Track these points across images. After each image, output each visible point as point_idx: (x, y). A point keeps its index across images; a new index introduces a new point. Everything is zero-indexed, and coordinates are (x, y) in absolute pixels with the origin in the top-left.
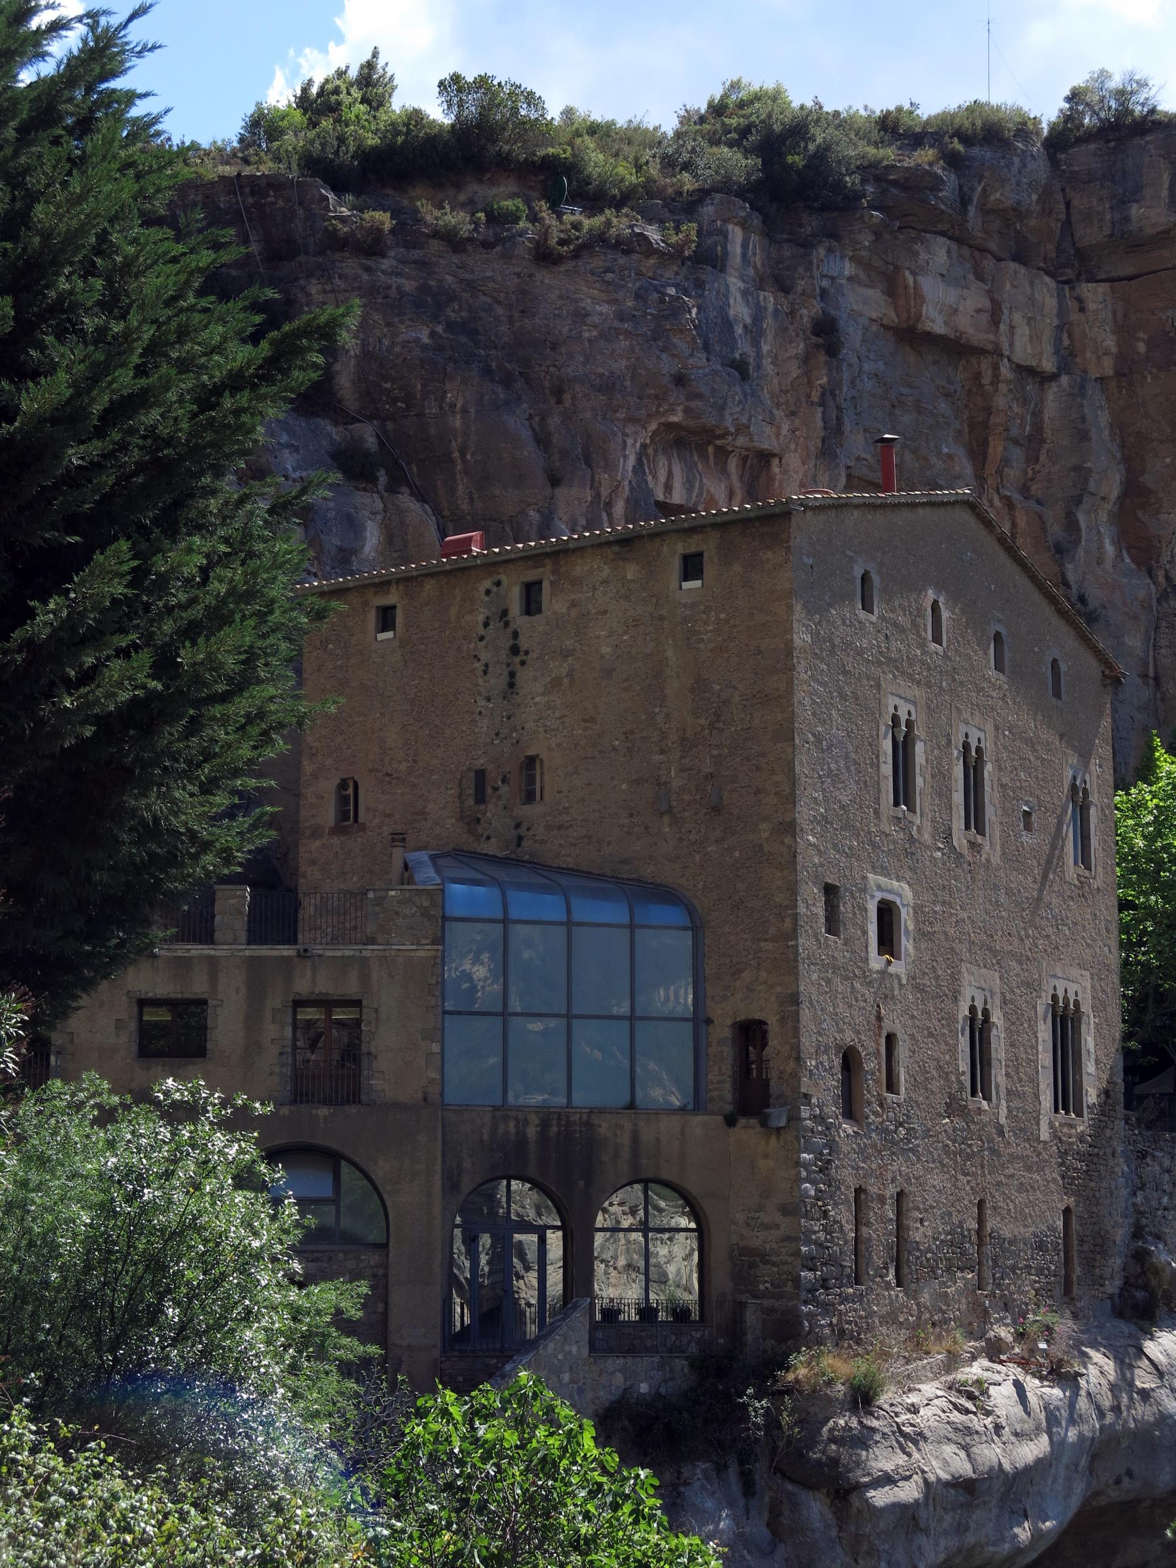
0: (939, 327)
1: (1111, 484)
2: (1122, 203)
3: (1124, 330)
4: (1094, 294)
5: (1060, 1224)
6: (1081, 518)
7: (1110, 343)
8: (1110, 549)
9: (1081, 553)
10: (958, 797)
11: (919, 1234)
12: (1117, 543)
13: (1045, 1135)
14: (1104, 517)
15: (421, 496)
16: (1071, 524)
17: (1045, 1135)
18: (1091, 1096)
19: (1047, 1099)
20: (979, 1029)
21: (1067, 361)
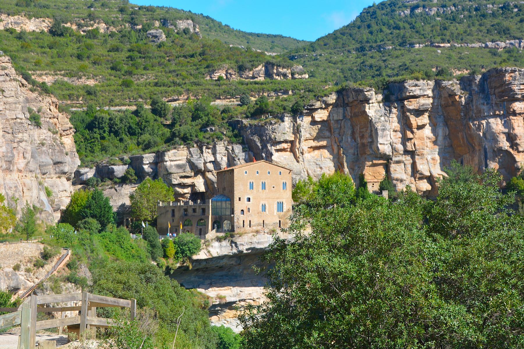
0: (319, 120)
1: (350, 132)
2: (348, 98)
3: (351, 113)
4: (348, 108)
5: (278, 222)
6: (344, 138)
7: (350, 114)
8: (349, 140)
9: (343, 141)
10: (261, 187)
11: (251, 223)
12: (351, 139)
13: (275, 214)
14: (349, 136)
15: (252, 151)
16: (342, 139)
17: (275, 214)
18: (284, 210)
19: (276, 211)
20: (264, 207)
21: (344, 117)
